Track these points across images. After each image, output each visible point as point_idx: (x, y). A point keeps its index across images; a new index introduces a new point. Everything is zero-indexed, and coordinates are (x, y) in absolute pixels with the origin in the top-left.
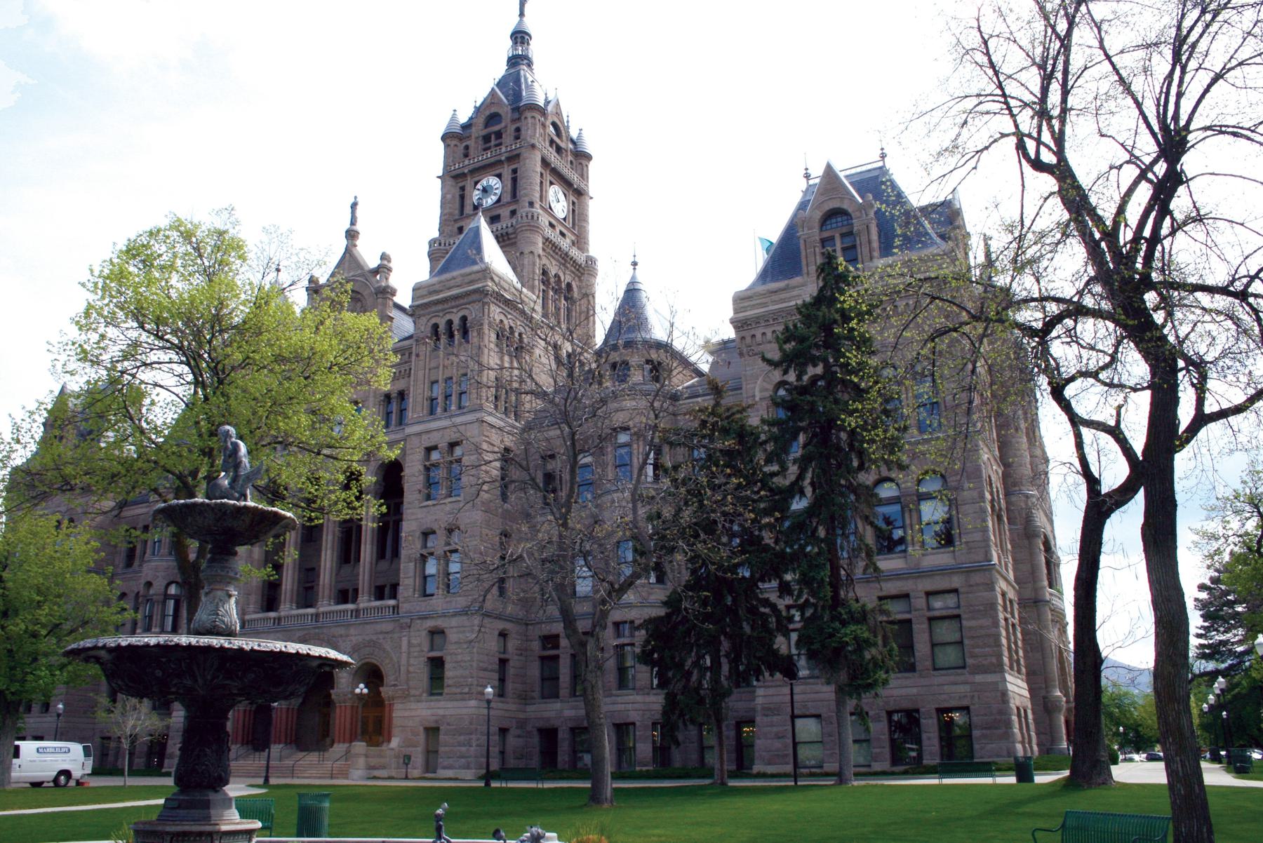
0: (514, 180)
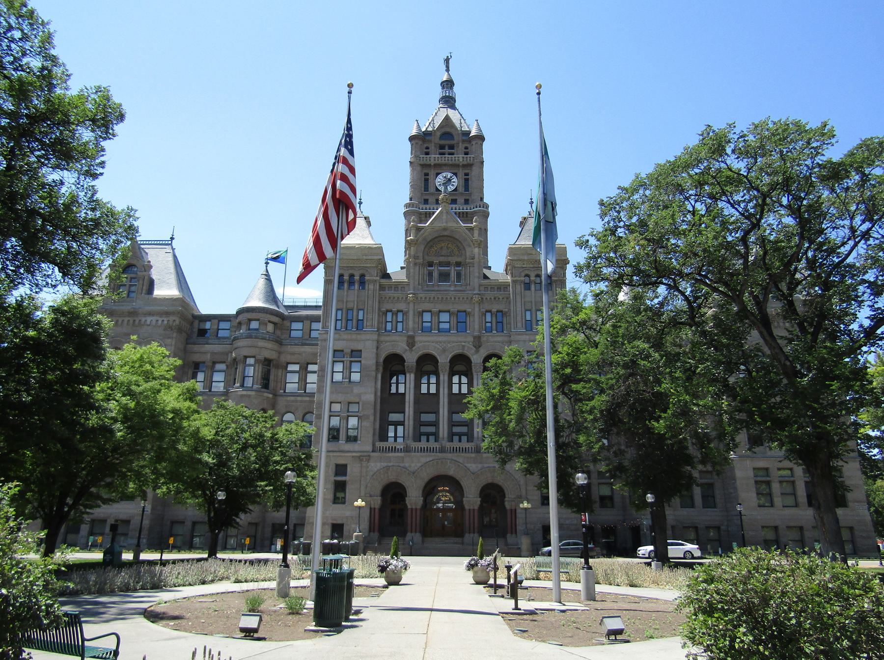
0: (467, 180)
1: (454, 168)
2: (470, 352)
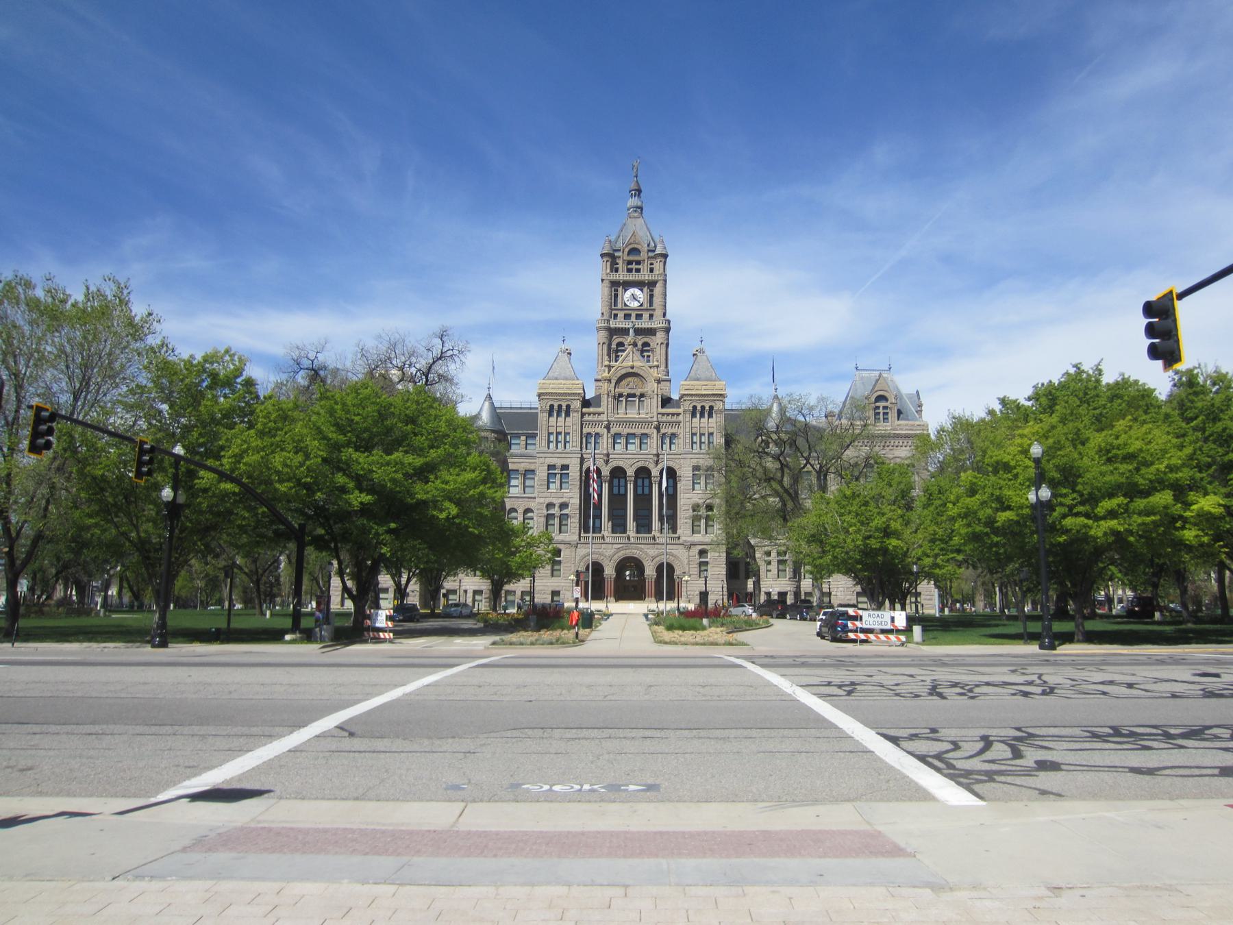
1: (639, 285)
2: (651, 466)
